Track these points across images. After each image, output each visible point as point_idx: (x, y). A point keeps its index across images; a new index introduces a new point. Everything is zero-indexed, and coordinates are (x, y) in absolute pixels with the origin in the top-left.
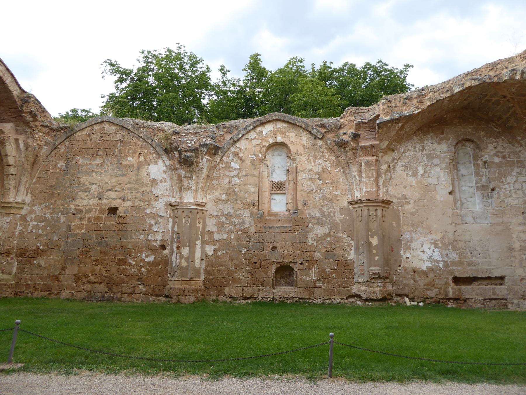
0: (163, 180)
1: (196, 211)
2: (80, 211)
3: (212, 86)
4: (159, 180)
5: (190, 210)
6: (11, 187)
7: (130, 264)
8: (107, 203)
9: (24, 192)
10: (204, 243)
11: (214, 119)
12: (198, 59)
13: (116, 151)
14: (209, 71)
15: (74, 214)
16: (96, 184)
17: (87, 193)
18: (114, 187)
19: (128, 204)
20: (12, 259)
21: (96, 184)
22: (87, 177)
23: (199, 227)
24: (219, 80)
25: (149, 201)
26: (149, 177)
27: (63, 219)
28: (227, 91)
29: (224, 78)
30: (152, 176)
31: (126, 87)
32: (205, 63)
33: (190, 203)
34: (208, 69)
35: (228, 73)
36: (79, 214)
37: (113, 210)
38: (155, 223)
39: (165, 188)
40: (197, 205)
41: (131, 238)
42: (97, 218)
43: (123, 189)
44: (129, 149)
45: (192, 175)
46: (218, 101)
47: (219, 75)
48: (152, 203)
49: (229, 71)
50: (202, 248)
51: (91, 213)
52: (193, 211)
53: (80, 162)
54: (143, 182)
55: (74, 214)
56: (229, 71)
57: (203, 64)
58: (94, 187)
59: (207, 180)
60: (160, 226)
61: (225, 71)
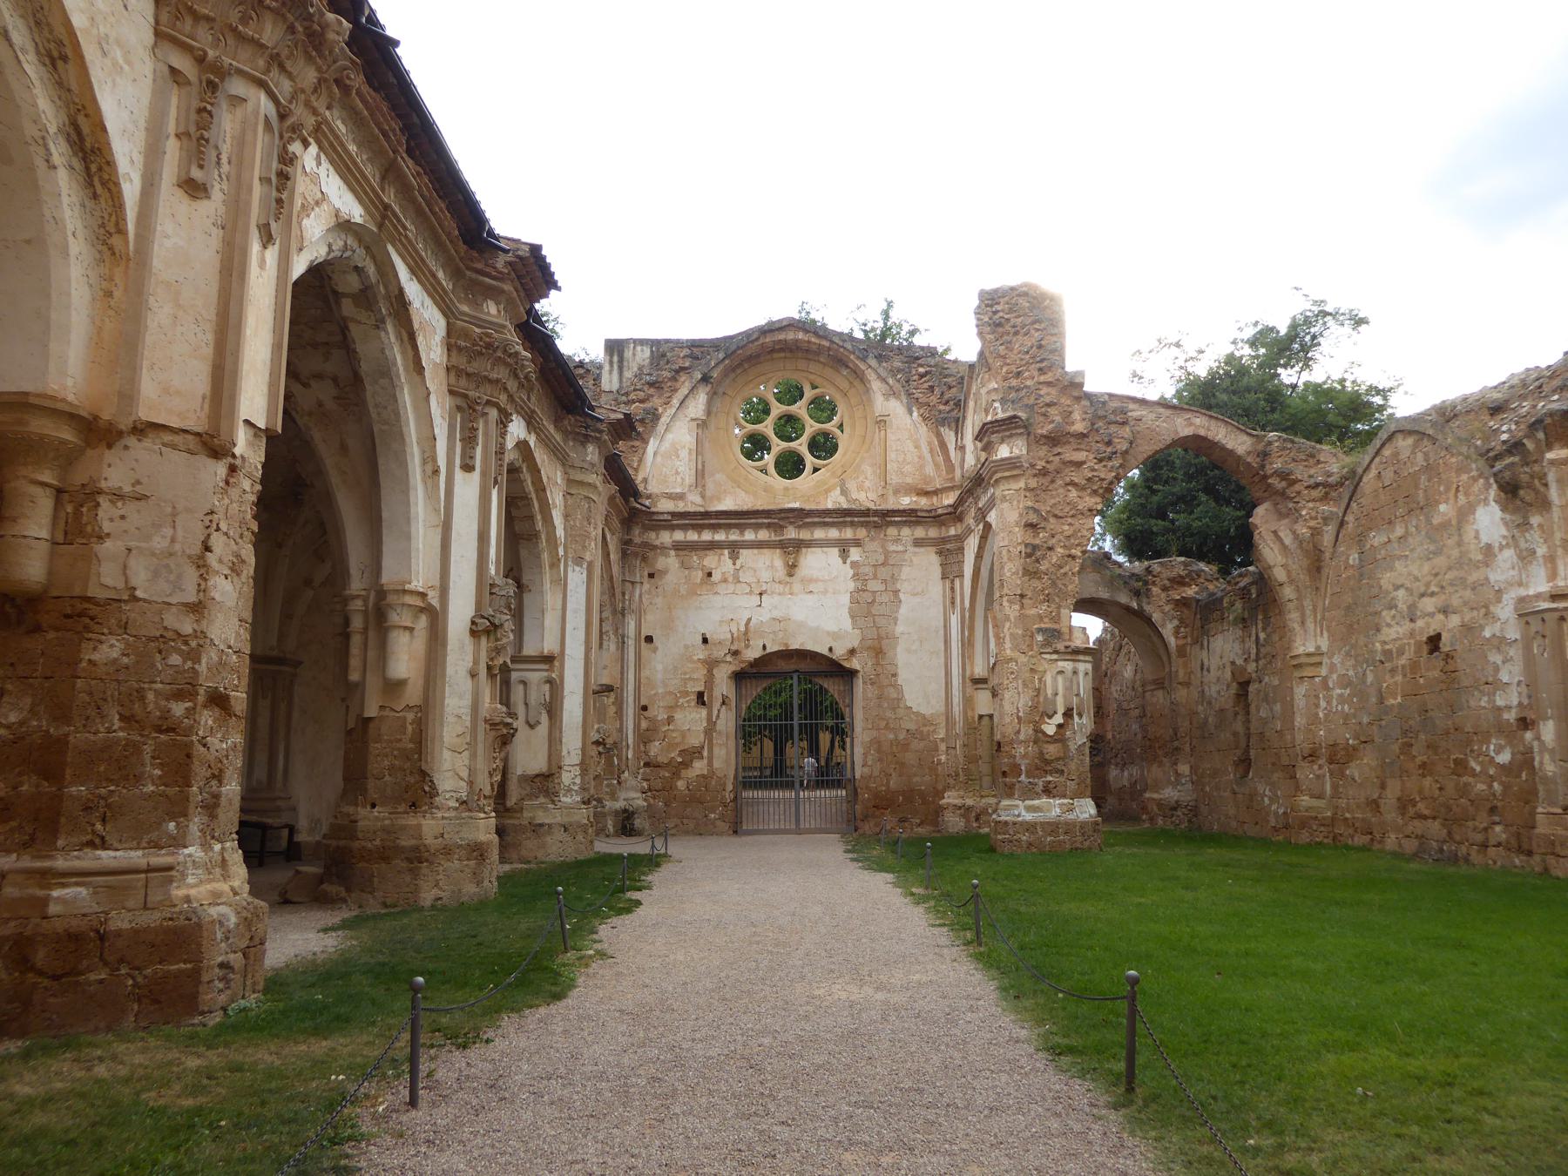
0: (1504, 543)
1: (1557, 615)
2: (1388, 653)
5: (1540, 616)
7: (1473, 774)
8: (1435, 624)
9: (1315, 630)
17: (1393, 612)
18: (1428, 585)
19: (1455, 620)
20: (1320, 767)
21: (1402, 586)
22: (1388, 575)
25: (1486, 607)
26: (1480, 542)
30: (1484, 539)
33: (1538, 596)
36: (1389, 661)
37: (1434, 642)
38: (1504, 662)
39: (1509, 563)
41: (1469, 707)
42: (1414, 666)
43: (1442, 587)
48: (1492, 608)
51: (1404, 657)
52: (1546, 616)
54: (1470, 560)
58: (1401, 593)
60: (1511, 668)
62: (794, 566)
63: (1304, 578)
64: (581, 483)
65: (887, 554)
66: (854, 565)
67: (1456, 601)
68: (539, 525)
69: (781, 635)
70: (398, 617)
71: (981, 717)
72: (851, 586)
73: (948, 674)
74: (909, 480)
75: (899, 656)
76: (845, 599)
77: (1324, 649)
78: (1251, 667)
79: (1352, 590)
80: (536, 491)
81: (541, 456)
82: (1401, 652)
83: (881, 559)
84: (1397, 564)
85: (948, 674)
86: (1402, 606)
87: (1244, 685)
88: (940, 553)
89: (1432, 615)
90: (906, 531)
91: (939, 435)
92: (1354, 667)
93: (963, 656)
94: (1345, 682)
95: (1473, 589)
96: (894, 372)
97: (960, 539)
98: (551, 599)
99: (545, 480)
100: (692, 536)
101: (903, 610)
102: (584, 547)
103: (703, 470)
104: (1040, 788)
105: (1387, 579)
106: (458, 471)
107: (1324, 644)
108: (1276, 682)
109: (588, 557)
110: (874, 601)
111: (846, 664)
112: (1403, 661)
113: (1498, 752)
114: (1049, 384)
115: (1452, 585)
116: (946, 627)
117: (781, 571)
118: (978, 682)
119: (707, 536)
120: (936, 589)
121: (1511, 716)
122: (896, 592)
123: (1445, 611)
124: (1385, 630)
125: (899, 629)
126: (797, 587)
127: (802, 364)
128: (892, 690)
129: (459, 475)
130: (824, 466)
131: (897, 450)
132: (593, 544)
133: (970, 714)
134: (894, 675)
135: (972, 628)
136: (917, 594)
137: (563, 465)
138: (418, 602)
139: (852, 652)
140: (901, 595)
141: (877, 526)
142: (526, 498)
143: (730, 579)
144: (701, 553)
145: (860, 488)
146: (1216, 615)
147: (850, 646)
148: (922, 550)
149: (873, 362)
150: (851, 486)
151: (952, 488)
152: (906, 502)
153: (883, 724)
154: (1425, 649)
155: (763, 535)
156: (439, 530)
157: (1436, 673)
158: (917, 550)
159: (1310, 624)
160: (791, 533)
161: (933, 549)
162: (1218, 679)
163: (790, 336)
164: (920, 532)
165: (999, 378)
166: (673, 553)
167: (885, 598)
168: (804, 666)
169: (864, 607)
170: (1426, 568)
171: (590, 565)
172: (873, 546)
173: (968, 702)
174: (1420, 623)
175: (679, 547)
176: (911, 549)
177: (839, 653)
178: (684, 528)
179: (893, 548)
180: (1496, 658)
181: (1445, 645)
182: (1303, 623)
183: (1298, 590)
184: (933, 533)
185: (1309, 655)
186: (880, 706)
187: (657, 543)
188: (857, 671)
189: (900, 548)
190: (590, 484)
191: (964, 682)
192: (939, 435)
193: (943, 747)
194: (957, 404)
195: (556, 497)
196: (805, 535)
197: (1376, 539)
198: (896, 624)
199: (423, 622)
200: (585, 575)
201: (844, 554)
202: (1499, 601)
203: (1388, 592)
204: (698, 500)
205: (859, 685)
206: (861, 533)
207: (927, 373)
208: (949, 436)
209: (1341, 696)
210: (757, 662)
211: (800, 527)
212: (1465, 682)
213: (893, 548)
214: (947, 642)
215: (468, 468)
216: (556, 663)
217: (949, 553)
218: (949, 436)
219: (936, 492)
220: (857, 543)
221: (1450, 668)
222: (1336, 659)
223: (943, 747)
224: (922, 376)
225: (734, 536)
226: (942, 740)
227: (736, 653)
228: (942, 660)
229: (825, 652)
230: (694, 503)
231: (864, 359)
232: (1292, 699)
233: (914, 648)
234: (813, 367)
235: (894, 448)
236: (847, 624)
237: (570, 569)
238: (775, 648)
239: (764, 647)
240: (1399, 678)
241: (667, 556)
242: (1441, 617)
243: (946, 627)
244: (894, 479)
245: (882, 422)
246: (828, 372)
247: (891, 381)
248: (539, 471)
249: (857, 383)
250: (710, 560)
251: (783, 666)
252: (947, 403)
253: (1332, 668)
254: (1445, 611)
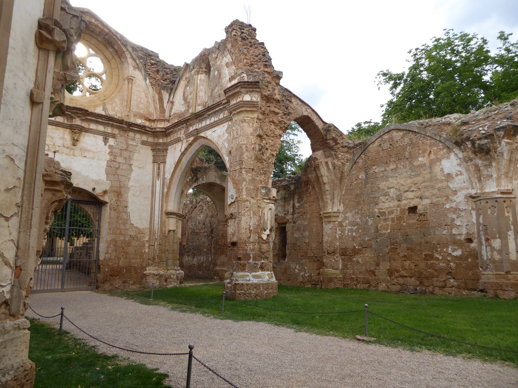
2: (383, 214)
3: (493, 58)
4: (454, 174)
6: (329, 201)
11: (504, 94)
12: (470, 36)
13: (407, 154)
14: (486, 44)
15: (379, 217)
16: (393, 187)
17: (387, 197)
21: (393, 187)
24: (500, 48)
27: (370, 222)
28: (513, 57)
29: (507, 44)
31: (401, 91)
32: (479, 37)
34: (485, 41)
35: (510, 37)
36: (383, 216)
40: (502, 193)
44: (419, 150)
45: (491, 163)
46: (503, 72)
47: (500, 43)
49: (511, 34)
53: (377, 170)
55: (379, 217)
56: (511, 34)
57: (478, 39)
58: (392, 190)
59: (510, 164)
61: (506, 36)
75: (129, 197)
90: (138, 136)
101: (133, 175)
110: (119, 167)
111: (102, 198)
116: (153, 186)
122: (131, 165)
125: (131, 184)
131: (137, 96)
136: (140, 168)
139: (105, 192)
140: (133, 167)
147: (104, 189)
148: (145, 147)
158: (142, 146)
167: (124, 167)
176: (140, 146)
177: (98, 192)
188: (106, 203)
189: (134, 144)
198: (129, 181)
233: (137, 194)
235: (136, 94)
244: (134, 109)
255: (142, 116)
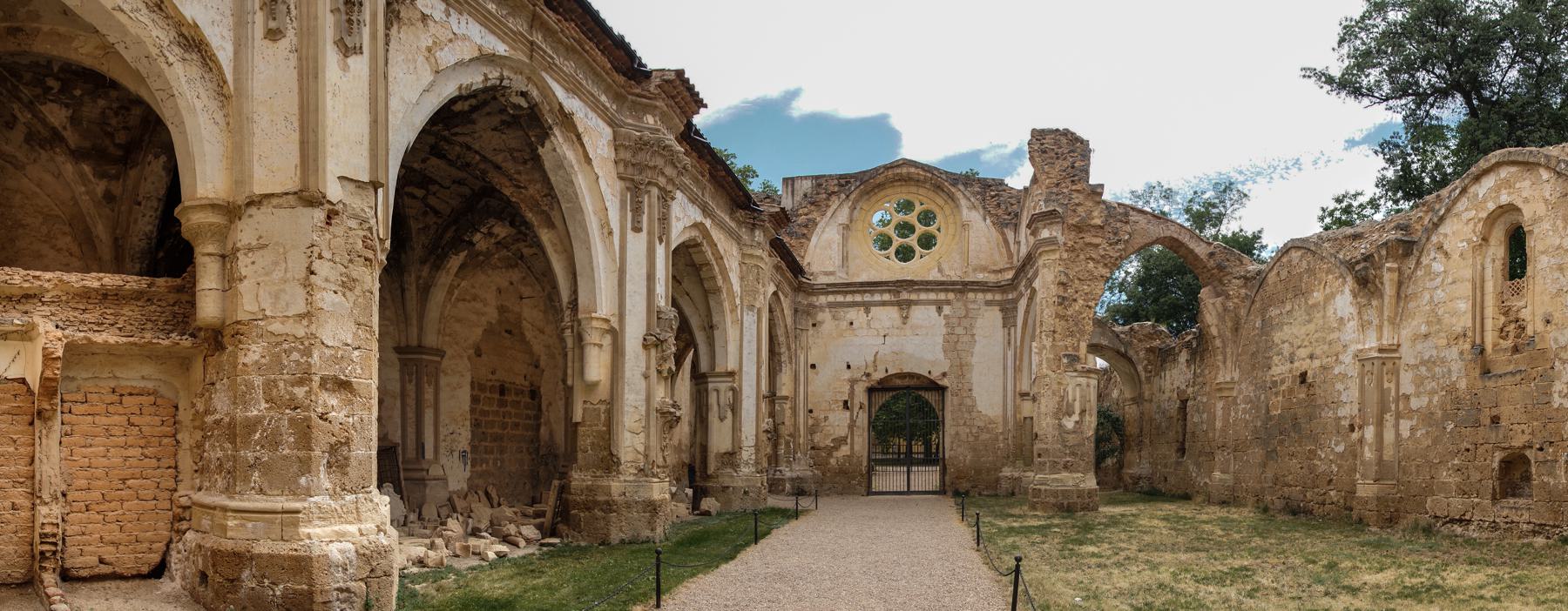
8: (1300, 366)
10: (1398, 416)
18: (1303, 340)
19: (1317, 363)
23: (1389, 389)
25: (1337, 355)
33: (1370, 349)
37: (1303, 376)
42: (1291, 391)
48: (1340, 357)
50: (1397, 426)
58: (1286, 345)
62: (907, 317)
63: (1228, 334)
64: (751, 256)
65: (967, 310)
66: (946, 317)
67: (1318, 352)
68: (720, 282)
69: (897, 362)
70: (592, 337)
71: (1025, 418)
72: (944, 331)
73: (1005, 389)
74: (983, 263)
76: (940, 340)
77: (1236, 379)
78: (1190, 390)
79: (1257, 343)
80: (716, 259)
81: (717, 235)
82: (1283, 382)
83: (964, 313)
84: (1285, 327)
85: (1005, 389)
86: (1286, 354)
87: (1184, 402)
88: (1001, 310)
89: (1303, 359)
90: (980, 296)
91: (1003, 234)
92: (1254, 391)
93: (1015, 377)
94: (1248, 400)
95: (1330, 344)
96: (975, 194)
97: (1015, 301)
98: (732, 333)
99: (722, 252)
100: (840, 298)
101: (977, 348)
102: (755, 299)
103: (847, 257)
104: (1060, 466)
105: (1277, 336)
106: (629, 232)
107: (1236, 376)
108: (1205, 400)
109: (758, 305)
111: (940, 383)
112: (1283, 388)
113: (1336, 445)
114: (1078, 191)
115: (1317, 341)
116: (1005, 358)
117: (898, 322)
118: (1024, 395)
119: (849, 298)
120: (1000, 333)
121: (1345, 423)
122: (973, 335)
123: (1311, 357)
124: (1274, 368)
125: (974, 360)
126: (908, 332)
127: (914, 189)
128: (968, 400)
129: (630, 235)
130: (928, 254)
132: (762, 297)
133: (1018, 416)
134: (970, 390)
135: (1021, 360)
137: (739, 244)
138: (605, 326)
139: (944, 375)
140: (977, 338)
141: (961, 292)
142: (708, 264)
143: (865, 326)
144: (846, 310)
145: (951, 268)
146: (1171, 358)
148: (990, 308)
149: (962, 188)
150: (945, 266)
151: (1011, 268)
152: (980, 277)
153: (962, 422)
154: (1298, 380)
155: (886, 297)
156: (616, 274)
157: (1303, 396)
159: (1229, 363)
160: (905, 296)
161: (998, 308)
162: (1170, 398)
163: (904, 170)
164: (989, 296)
165: (1043, 187)
166: (827, 310)
167: (965, 339)
168: (913, 382)
169: (952, 345)
170: (1303, 330)
171: (759, 310)
172: (959, 304)
173: (1017, 409)
174: (1296, 364)
175: (831, 305)
177: (935, 375)
178: (833, 293)
179: (971, 306)
180: (1339, 386)
181: (1309, 380)
182: (1225, 362)
183: (1223, 342)
184: (998, 297)
185: (1227, 383)
186: (960, 410)
187: (817, 304)
189: (976, 307)
190: (757, 256)
191: (1015, 396)
192: (1003, 234)
193: (1001, 438)
194: (1016, 215)
195: (733, 264)
196: (914, 297)
197: (1274, 312)
199: (607, 341)
200: (755, 318)
201: (939, 310)
202: (1345, 351)
203: (1277, 345)
204: (844, 276)
205: (948, 396)
206: (951, 296)
207: (996, 195)
208: (1010, 235)
209: (1244, 409)
210: (881, 381)
211: (910, 292)
212: (1320, 402)
213: (971, 306)
214: (1005, 368)
215: (637, 229)
216: (737, 377)
217: (1008, 311)
218: (1010, 235)
219: (1000, 271)
220: (948, 302)
221: (1311, 392)
222: (1244, 386)
223: (1001, 438)
224: (993, 197)
225: (867, 298)
226: (1001, 433)
227: (868, 375)
228: (1002, 381)
229: (926, 374)
230: (841, 277)
231: (954, 185)
232: (1215, 411)
234: (921, 191)
236: (941, 356)
237: (745, 314)
238: (895, 372)
239: (887, 371)
240: (1280, 398)
241: (824, 312)
242: (1308, 361)
243: (1005, 358)
245: (965, 226)
246: (931, 194)
247: (972, 199)
248: (716, 245)
249: (950, 201)
250: (852, 314)
251: (898, 382)
252: (1009, 214)
253: (1240, 392)
254: (1311, 357)
255: (984, 269)
